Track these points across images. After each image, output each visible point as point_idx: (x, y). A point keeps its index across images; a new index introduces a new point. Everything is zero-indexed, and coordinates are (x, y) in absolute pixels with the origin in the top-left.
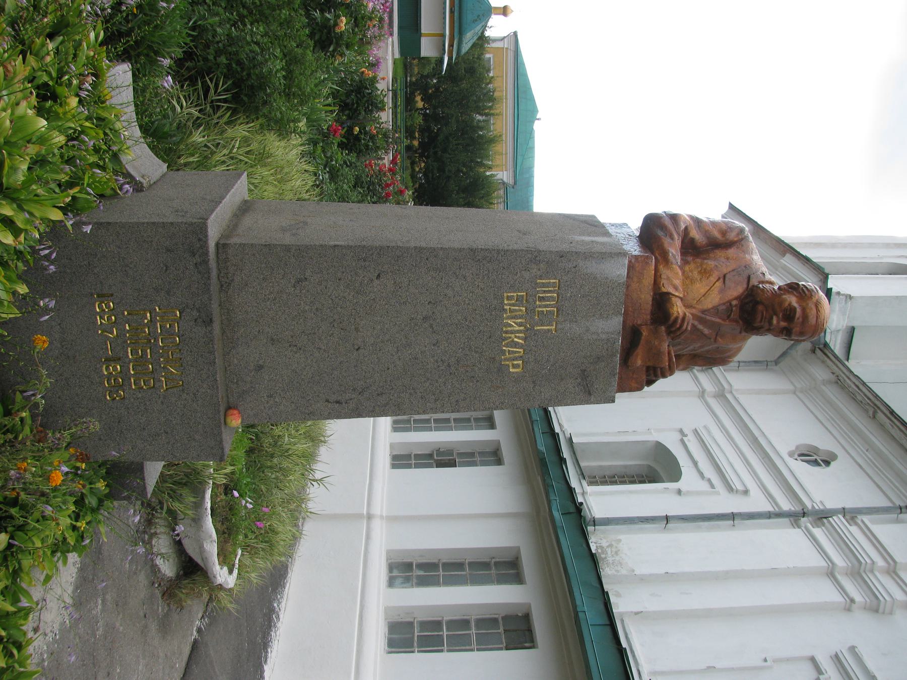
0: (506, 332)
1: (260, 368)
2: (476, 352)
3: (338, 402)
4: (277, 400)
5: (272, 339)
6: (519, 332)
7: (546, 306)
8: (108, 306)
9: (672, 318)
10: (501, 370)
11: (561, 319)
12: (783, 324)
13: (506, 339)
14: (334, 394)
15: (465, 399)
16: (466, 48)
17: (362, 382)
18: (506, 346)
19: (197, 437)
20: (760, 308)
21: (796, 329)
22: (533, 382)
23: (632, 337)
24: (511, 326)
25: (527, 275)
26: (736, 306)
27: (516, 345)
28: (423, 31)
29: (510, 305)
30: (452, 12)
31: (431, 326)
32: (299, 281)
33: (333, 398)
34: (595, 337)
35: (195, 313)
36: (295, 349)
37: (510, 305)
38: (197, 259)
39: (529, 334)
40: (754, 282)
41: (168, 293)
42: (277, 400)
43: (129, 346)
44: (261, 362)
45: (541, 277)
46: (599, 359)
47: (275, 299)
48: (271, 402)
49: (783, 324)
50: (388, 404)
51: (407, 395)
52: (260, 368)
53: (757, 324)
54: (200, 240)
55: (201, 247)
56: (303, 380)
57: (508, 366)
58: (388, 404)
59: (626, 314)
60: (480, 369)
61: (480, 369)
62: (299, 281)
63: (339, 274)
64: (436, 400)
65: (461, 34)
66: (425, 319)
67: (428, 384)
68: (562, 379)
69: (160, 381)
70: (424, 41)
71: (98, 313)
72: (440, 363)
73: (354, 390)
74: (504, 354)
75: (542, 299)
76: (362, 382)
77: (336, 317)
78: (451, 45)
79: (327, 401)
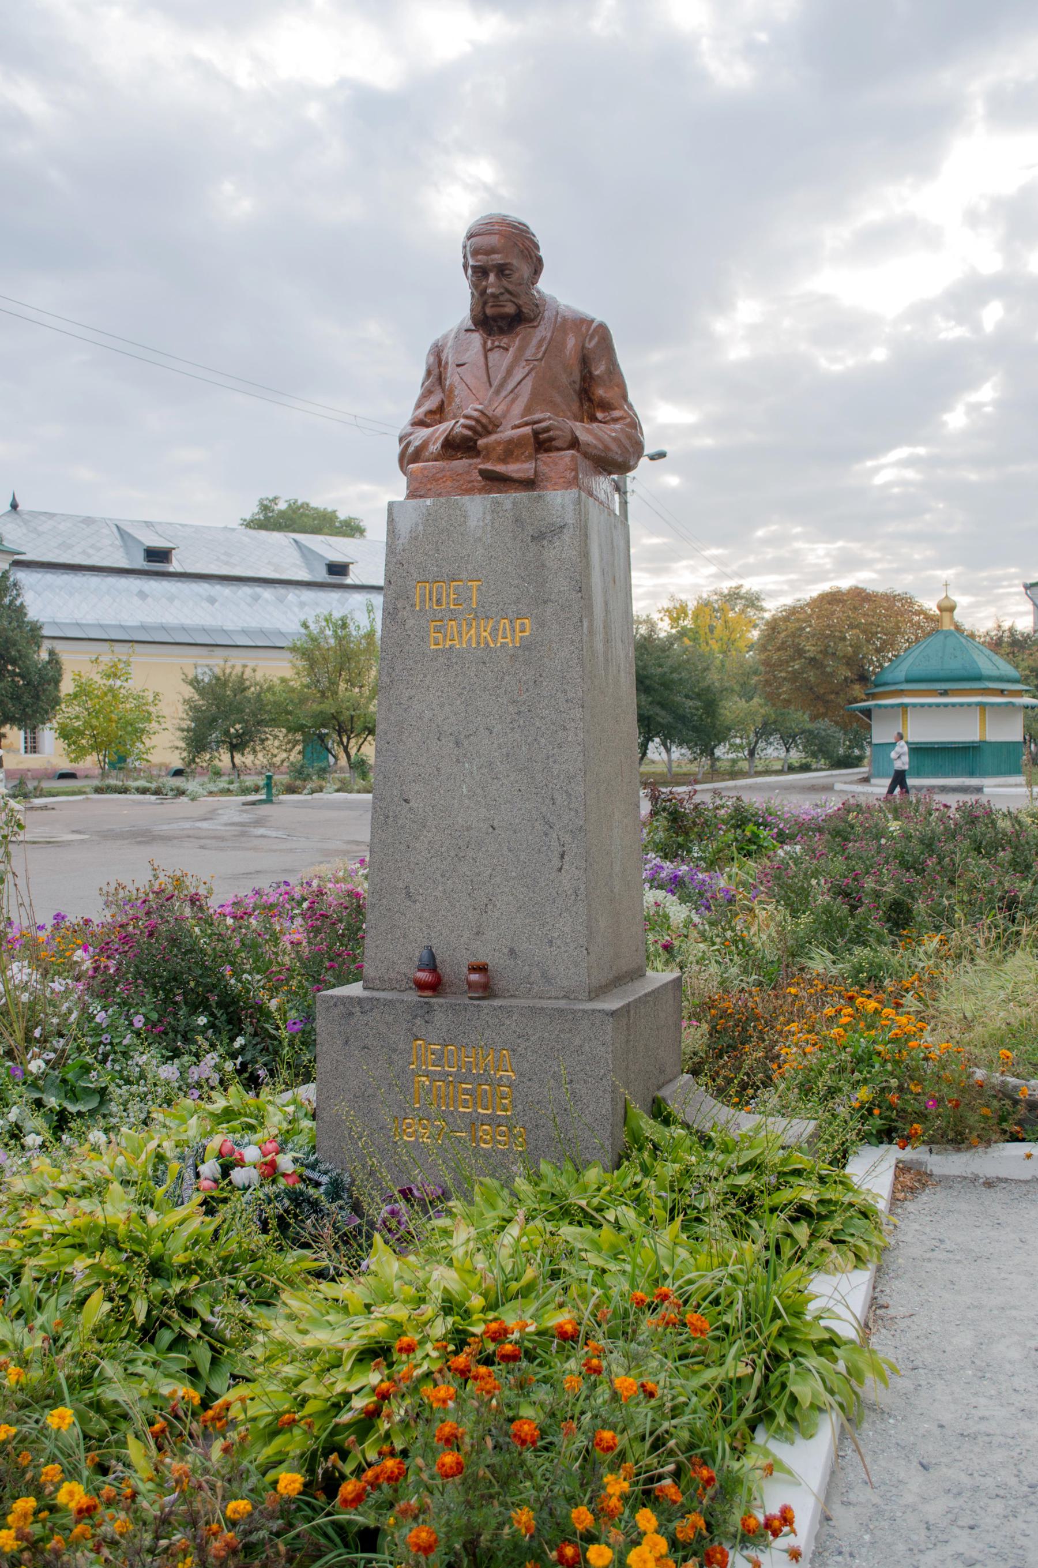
0: (478, 643)
1: (512, 952)
2: (502, 679)
3: (562, 856)
4: (556, 935)
5: (477, 934)
6: (478, 627)
7: (448, 596)
8: (410, 1126)
9: (469, 433)
10: (527, 646)
11: (464, 576)
12: (492, 278)
13: (487, 644)
14: (550, 861)
15: (565, 691)
16: (1006, 669)
17: (537, 824)
18: (495, 641)
19: (577, 1042)
20: (489, 311)
21: (497, 258)
22: (545, 602)
23: (495, 481)
24: (470, 638)
25: (411, 623)
26: (493, 342)
27: (495, 629)
28: (977, 739)
29: (445, 640)
30: (945, 693)
31: (467, 737)
32: (409, 895)
33: (556, 862)
34: (489, 528)
35: (419, 1021)
36: (490, 907)
37: (445, 640)
38: (357, 1010)
39: (481, 614)
40: (469, 324)
41: (394, 1050)
42: (556, 935)
43: (456, 1109)
44: (506, 951)
45: (413, 606)
46: (518, 521)
47: (429, 926)
48: (559, 942)
49: (492, 278)
50: (567, 792)
51: (557, 766)
52: (512, 952)
53: (510, 309)
54: (335, 1005)
55: (344, 1004)
56: (530, 899)
57: (521, 638)
58: (567, 792)
59: (468, 491)
60: (525, 674)
61: (525, 674)
62: (409, 895)
63: (403, 848)
64: (565, 729)
65: (979, 678)
66: (458, 744)
67: (543, 740)
68: (543, 565)
69: (501, 1077)
70: (991, 737)
71: (417, 1139)
72: (516, 725)
73: (546, 834)
74: (507, 643)
75: (439, 602)
76: (537, 824)
77: (452, 854)
78: (1002, 692)
79: (560, 870)
